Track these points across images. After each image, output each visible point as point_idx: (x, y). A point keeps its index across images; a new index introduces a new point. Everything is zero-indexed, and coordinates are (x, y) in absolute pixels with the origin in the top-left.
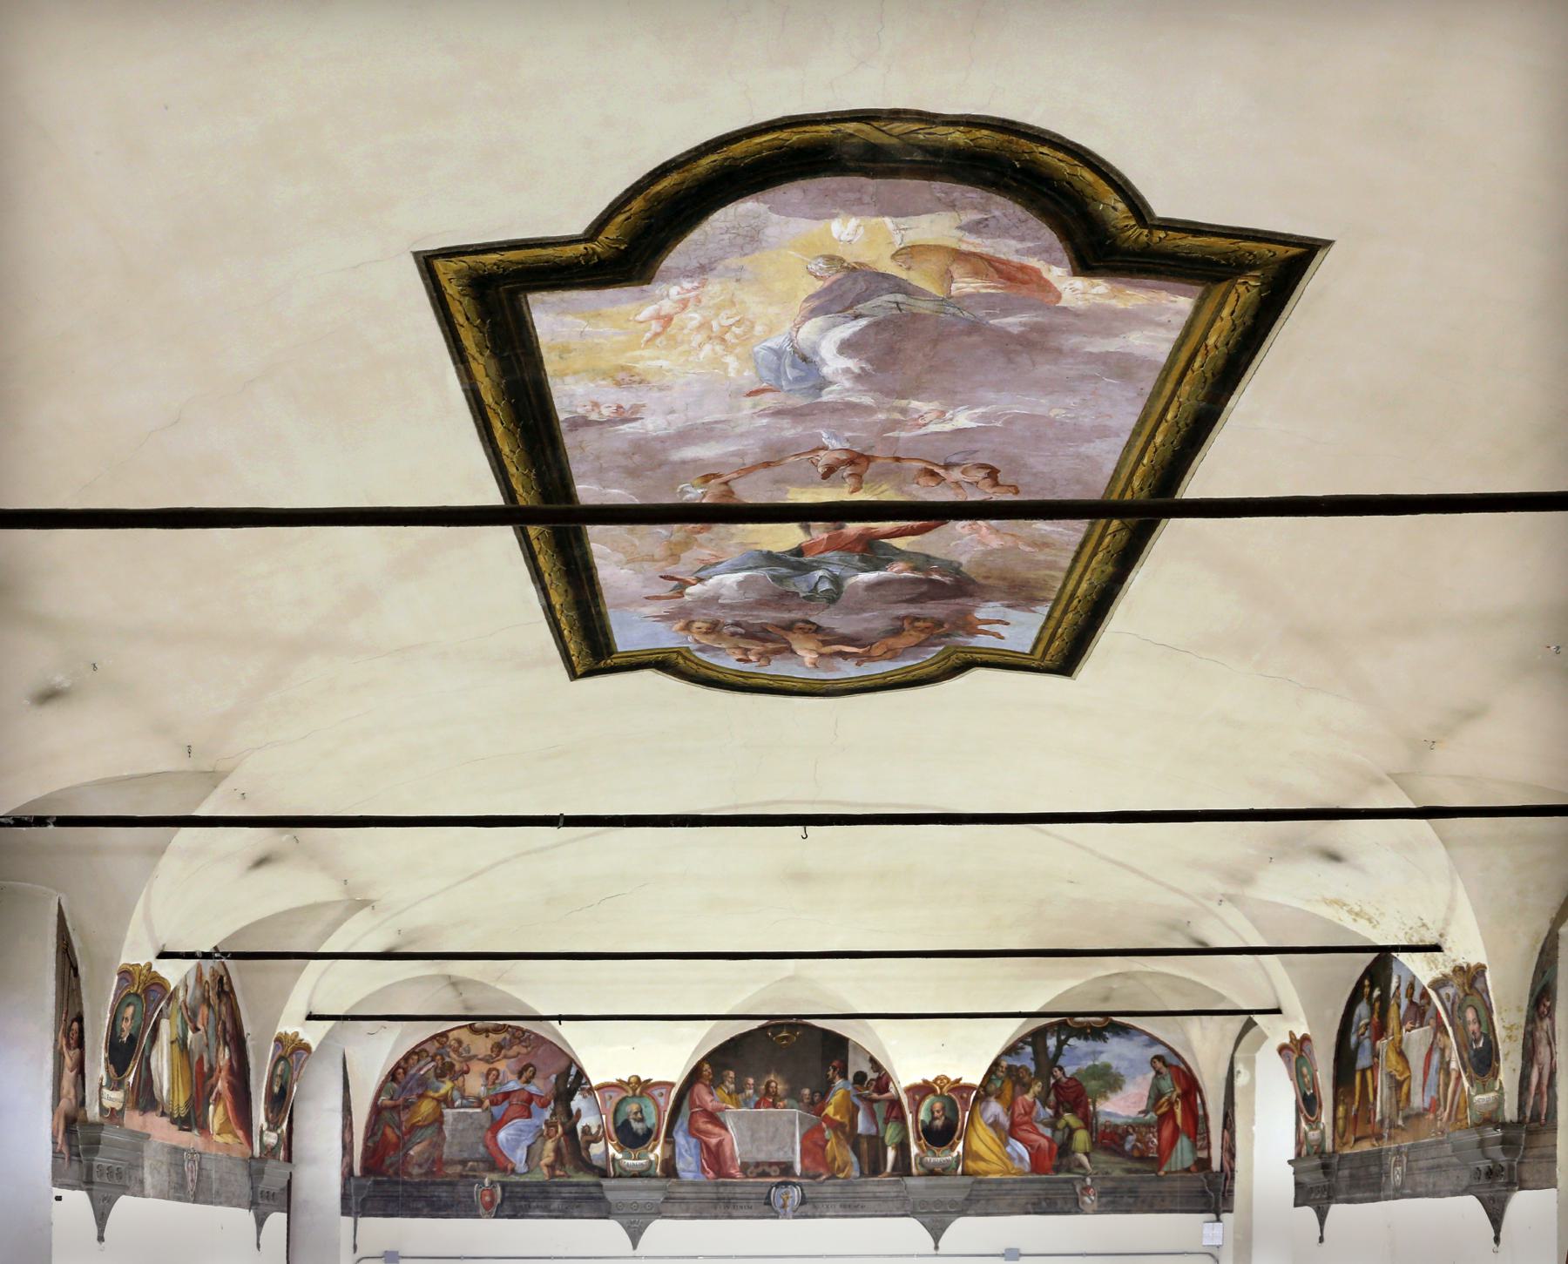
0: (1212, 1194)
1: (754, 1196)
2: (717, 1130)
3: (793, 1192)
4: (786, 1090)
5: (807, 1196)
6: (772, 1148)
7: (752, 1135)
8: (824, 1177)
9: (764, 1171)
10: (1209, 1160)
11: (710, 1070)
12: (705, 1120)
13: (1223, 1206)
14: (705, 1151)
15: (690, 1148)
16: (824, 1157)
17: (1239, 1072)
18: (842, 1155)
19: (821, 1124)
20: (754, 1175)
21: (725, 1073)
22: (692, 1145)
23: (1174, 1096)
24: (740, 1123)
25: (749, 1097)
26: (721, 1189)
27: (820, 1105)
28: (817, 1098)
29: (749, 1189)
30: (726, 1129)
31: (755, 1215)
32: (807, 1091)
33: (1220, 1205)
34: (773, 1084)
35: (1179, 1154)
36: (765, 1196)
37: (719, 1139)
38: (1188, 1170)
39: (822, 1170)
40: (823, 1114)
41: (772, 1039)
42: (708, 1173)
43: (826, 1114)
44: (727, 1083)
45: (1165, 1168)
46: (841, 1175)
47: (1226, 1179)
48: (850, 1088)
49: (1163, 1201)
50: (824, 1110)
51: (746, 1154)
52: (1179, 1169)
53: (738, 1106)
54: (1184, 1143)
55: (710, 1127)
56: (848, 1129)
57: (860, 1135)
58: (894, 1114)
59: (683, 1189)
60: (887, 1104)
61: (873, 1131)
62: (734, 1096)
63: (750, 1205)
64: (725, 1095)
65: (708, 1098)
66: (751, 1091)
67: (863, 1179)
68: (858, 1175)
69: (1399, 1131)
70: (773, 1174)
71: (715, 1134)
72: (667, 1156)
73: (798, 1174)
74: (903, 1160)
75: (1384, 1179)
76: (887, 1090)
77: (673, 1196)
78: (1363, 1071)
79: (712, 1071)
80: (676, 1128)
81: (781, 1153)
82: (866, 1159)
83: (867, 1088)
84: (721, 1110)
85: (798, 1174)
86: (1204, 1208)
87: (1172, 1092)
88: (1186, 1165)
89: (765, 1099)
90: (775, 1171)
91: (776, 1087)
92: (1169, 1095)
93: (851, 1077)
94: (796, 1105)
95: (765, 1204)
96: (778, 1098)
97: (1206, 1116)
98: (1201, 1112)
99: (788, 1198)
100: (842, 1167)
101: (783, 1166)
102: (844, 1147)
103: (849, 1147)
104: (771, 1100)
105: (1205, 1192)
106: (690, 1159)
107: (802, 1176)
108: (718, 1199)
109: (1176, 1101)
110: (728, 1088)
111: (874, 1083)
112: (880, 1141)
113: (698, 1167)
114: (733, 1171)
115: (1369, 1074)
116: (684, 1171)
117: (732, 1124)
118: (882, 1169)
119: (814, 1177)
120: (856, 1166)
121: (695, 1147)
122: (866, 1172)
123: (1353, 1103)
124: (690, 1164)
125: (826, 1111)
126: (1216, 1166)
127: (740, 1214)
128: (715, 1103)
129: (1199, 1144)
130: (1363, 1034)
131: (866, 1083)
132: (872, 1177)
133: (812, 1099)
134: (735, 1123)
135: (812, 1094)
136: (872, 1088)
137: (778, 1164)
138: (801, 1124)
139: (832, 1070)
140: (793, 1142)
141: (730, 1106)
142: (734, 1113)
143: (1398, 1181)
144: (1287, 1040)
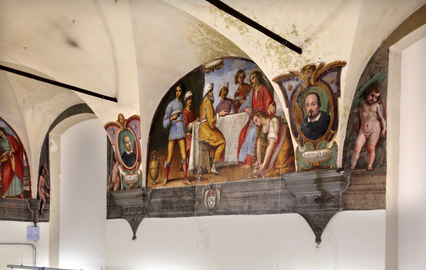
0: (32, 211)
10: (30, 192)
13: (39, 218)
17: (52, 144)
23: (11, 153)
33: (37, 218)
35: (14, 186)
38: (19, 196)
45: (6, 194)
47: (42, 203)
49: (4, 213)
52: (14, 195)
54: (16, 181)
69: (213, 176)
75: (197, 203)
78: (176, 142)
86: (28, 219)
87: (9, 150)
88: (18, 194)
92: (8, 152)
97: (28, 167)
98: (25, 165)
105: (28, 210)
109: (12, 156)
115: (182, 143)
123: (166, 159)
126: (34, 195)
129: (25, 182)
130: (176, 119)
143: (212, 205)
144: (115, 120)
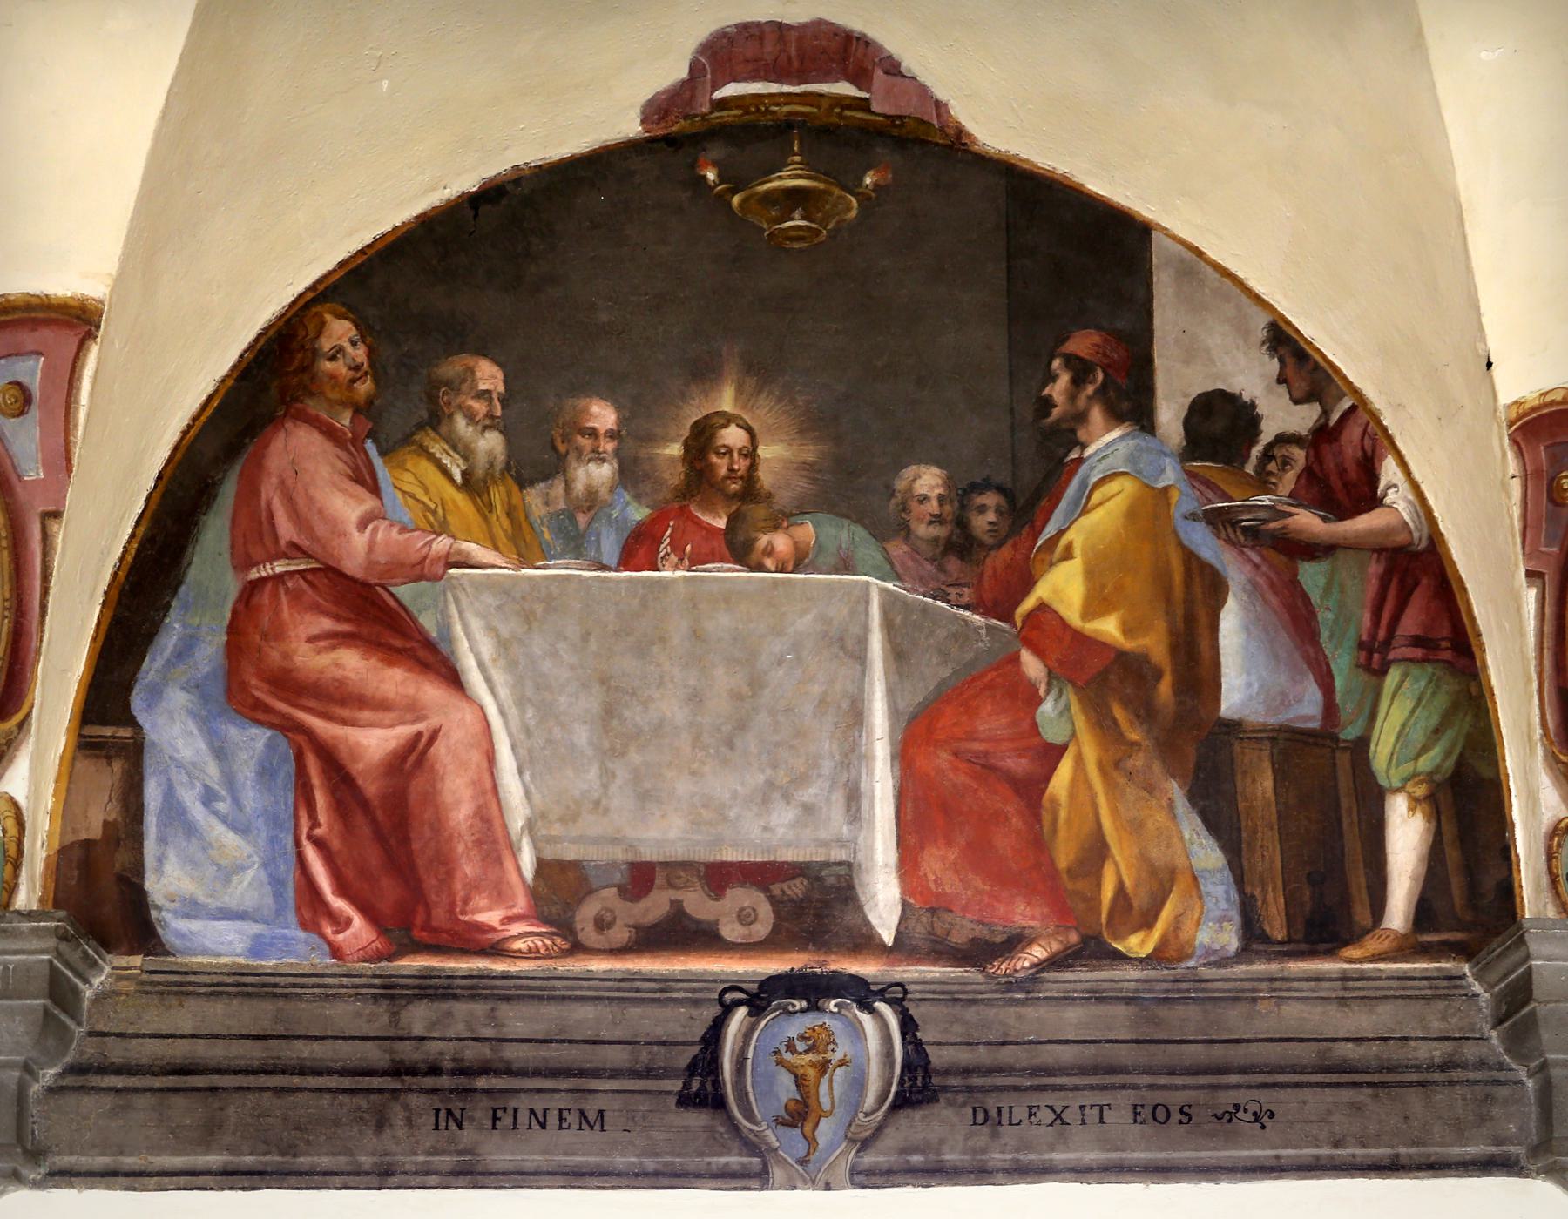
1: (617, 1056)
2: (394, 681)
3: (857, 1031)
4: (807, 467)
5: (938, 1057)
6: (722, 785)
7: (609, 712)
8: (1038, 952)
9: (678, 911)
11: (360, 354)
12: (327, 624)
14: (321, 800)
15: (229, 780)
16: (1039, 843)
18: (1136, 827)
19: (1015, 659)
20: (620, 935)
21: (450, 368)
22: (247, 773)
24: (538, 645)
25: (591, 502)
26: (418, 1017)
27: (1006, 553)
28: (986, 516)
29: (584, 1017)
30: (453, 678)
31: (620, 1161)
32: (928, 481)
34: (733, 436)
36: (684, 1057)
37: (405, 731)
39: (1023, 914)
40: (1028, 604)
41: (723, 200)
42: (349, 922)
43: (1043, 607)
44: (461, 423)
46: (1138, 944)
48: (1171, 474)
50: (1028, 583)
51: (570, 817)
53: (525, 549)
55: (352, 664)
56: (1165, 688)
57: (1233, 727)
58: (1410, 623)
59: (185, 1017)
60: (1375, 568)
61: (1307, 707)
62: (497, 495)
63: (592, 1106)
64: (450, 492)
65: (346, 506)
66: (600, 473)
67: (1259, 967)
68: (1230, 940)
70: (731, 931)
71: (383, 705)
72: (96, 817)
73: (888, 937)
74: (1471, 870)
76: (1368, 498)
77: (117, 1052)
79: (371, 353)
80: (152, 667)
81: (783, 817)
82: (1268, 854)
83: (1263, 483)
84: (420, 571)
85: (888, 937)
89: (683, 512)
90: (746, 917)
91: (751, 454)
93: (1170, 415)
94: (868, 550)
95: (686, 1100)
96: (758, 512)
99: (823, 1067)
100: (1140, 900)
101: (797, 888)
102: (1150, 789)
103: (1175, 790)
104: (721, 523)
106: (230, 839)
107: (903, 948)
108: (398, 1070)
110: (466, 453)
111: (1299, 455)
112: (1343, 760)
113: (276, 882)
114: (491, 917)
116: (192, 909)
117: (487, 648)
118: (1362, 915)
119: (979, 953)
120: (1219, 893)
121: (266, 773)
122: (1276, 928)
124: (228, 873)
125: (1042, 591)
127: (534, 1160)
128: (385, 534)
131: (1256, 451)
132: (1312, 954)
133: (962, 523)
134: (503, 645)
135: (962, 493)
136: (1288, 481)
137: (761, 875)
138: (898, 655)
139: (1064, 380)
140: (853, 755)
141: (472, 548)
142: (503, 589)
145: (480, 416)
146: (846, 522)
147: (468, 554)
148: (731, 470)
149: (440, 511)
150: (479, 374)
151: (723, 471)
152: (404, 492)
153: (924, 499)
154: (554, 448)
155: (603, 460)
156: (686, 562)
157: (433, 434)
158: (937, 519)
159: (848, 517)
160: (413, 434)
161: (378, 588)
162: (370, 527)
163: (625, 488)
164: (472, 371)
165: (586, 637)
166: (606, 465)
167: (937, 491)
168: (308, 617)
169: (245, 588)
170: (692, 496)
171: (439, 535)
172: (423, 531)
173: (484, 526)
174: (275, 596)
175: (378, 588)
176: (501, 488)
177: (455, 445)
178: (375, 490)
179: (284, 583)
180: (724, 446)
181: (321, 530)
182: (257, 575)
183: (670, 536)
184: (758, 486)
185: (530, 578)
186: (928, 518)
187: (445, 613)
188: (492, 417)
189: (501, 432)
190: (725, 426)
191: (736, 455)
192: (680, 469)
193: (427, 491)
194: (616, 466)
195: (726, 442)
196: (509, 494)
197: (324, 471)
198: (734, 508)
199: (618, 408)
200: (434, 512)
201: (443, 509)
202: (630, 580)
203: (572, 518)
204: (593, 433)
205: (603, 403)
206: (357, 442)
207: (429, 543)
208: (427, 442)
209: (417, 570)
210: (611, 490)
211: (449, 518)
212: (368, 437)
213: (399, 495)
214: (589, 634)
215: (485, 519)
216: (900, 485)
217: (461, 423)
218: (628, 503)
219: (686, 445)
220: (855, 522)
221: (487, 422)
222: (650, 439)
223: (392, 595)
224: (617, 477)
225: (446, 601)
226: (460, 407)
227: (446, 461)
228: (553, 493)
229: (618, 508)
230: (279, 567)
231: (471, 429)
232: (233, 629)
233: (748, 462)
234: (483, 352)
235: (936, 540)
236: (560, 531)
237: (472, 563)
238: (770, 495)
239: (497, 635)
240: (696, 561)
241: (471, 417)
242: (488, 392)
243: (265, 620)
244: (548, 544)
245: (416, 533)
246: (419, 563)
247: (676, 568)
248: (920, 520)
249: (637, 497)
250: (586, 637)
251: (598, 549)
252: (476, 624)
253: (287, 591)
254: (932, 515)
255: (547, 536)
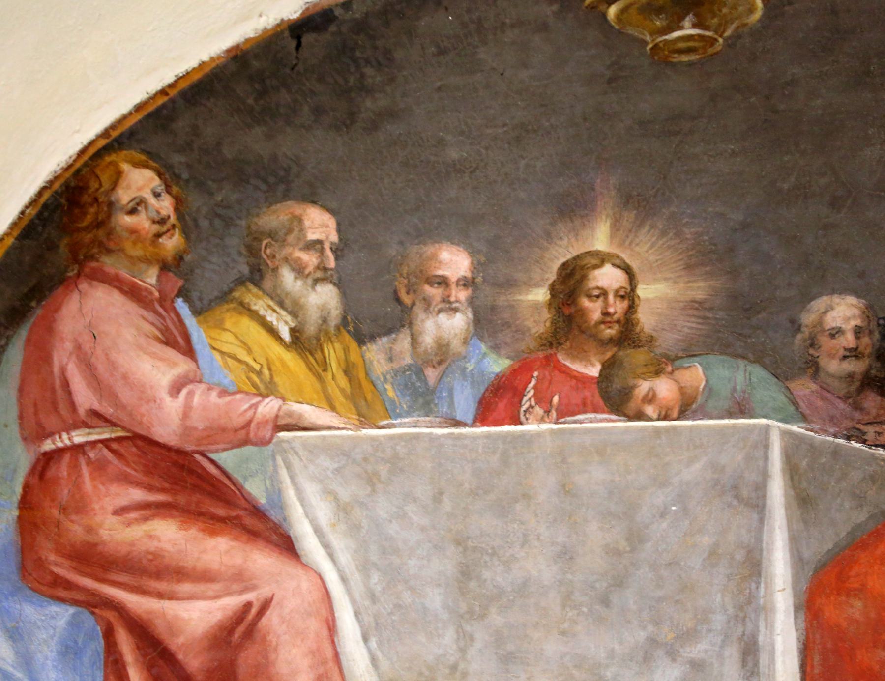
4: (696, 305)
12: (137, 495)
24: (383, 507)
44: (287, 277)
62: (333, 353)
64: (277, 350)
89: (549, 362)
91: (629, 295)
96: (637, 357)
104: (594, 371)
110: (295, 309)
117: (324, 512)
134: (343, 509)
145: (310, 269)
146: (742, 363)
147: (300, 416)
148: (606, 314)
149: (266, 372)
150: (307, 223)
151: (596, 316)
152: (222, 353)
153: (836, 333)
154: (398, 300)
155: (456, 310)
156: (554, 414)
157: (255, 290)
158: (854, 353)
159: (744, 357)
160: (231, 291)
161: (198, 457)
162: (184, 392)
163: (481, 339)
164: (300, 220)
165: (438, 497)
166: (459, 316)
167: (853, 323)
168: (114, 488)
169: (38, 461)
170: (560, 344)
171: (267, 396)
172: (247, 393)
173: (318, 386)
174: (75, 467)
175: (198, 457)
176: (337, 345)
177: (281, 301)
178: (189, 351)
179: (84, 453)
180: (598, 288)
181: (126, 396)
182: (53, 447)
183: (535, 388)
184: (638, 329)
185: (373, 439)
186: (842, 352)
187: (274, 478)
188: (325, 269)
189: (335, 284)
190: (596, 267)
191: (611, 297)
192: (546, 315)
193: (249, 351)
194: (470, 316)
195: (600, 284)
196: (346, 350)
197: (128, 334)
198: (609, 354)
199: (473, 252)
200: (259, 373)
201: (270, 369)
202: (488, 436)
203: (420, 372)
204: (443, 282)
205: (454, 248)
206: (166, 301)
207: (255, 406)
208: (248, 299)
209: (242, 434)
210: (466, 342)
211: (277, 379)
212: (178, 295)
213: (217, 356)
214: (441, 493)
215: (319, 378)
216: (808, 319)
217: (287, 277)
218: (485, 355)
219: (552, 288)
220: (751, 362)
221: (319, 274)
222: (510, 284)
223: (212, 462)
224: (472, 329)
225: (275, 466)
226: (286, 260)
227: (271, 318)
228: (397, 348)
229: (473, 361)
230: (79, 437)
231: (299, 283)
232: (26, 503)
233: (625, 304)
234: (313, 201)
235: (851, 376)
236: (406, 387)
237: (306, 425)
238: (651, 339)
239: (336, 499)
240: (564, 412)
241: (299, 270)
242: (320, 242)
243: (64, 493)
244: (393, 402)
245: (238, 396)
246: (243, 428)
247: (542, 420)
248: (832, 356)
249: (496, 348)
250: (438, 497)
251: (451, 404)
252: (311, 490)
253: (89, 462)
254: (845, 349)
255: (391, 393)
